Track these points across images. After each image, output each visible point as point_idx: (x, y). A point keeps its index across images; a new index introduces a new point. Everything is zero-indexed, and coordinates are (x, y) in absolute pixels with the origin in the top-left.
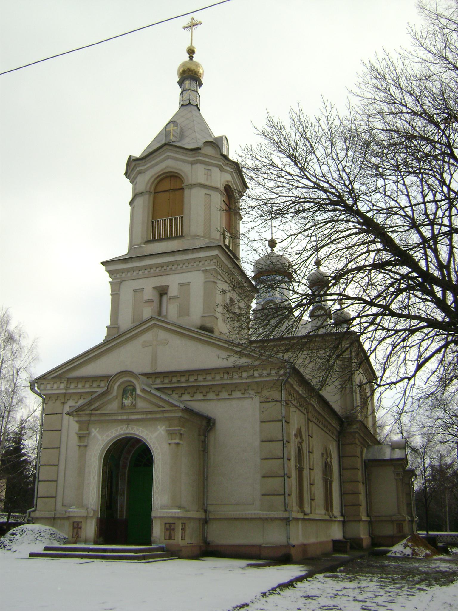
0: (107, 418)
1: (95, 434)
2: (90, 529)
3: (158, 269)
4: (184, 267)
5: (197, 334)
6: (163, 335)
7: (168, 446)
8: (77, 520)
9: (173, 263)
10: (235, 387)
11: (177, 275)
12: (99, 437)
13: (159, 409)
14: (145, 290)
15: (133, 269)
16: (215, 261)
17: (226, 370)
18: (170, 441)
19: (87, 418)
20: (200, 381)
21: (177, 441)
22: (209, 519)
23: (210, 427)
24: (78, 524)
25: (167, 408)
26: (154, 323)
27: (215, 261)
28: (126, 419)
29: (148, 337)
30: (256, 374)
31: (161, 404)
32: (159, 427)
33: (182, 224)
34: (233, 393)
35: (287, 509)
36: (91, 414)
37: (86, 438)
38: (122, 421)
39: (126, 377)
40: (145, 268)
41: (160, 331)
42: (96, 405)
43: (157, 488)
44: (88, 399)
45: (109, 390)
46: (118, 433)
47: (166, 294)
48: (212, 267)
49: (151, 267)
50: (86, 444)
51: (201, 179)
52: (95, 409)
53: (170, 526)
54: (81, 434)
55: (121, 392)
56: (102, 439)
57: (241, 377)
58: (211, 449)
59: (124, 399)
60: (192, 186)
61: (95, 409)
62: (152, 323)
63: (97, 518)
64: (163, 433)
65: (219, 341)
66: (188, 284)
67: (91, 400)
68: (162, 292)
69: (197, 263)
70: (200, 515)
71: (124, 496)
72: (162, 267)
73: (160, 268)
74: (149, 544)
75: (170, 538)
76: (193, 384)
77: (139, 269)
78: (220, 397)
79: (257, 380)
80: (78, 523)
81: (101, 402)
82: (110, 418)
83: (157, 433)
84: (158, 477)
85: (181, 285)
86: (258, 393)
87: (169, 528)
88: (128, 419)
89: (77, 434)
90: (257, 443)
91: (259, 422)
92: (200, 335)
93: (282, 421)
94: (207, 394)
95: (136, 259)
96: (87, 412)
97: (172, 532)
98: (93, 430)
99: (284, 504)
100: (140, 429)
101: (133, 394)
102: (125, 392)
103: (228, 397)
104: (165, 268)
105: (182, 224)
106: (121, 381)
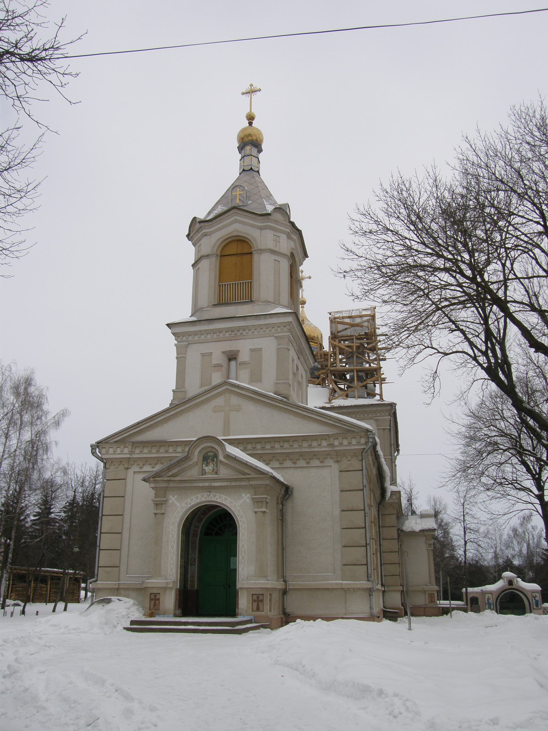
0: (187, 485)
1: (173, 501)
2: (169, 601)
3: (227, 334)
4: (256, 333)
5: (273, 401)
6: (235, 400)
7: (254, 514)
8: (155, 591)
9: (244, 328)
10: (315, 455)
11: (248, 340)
12: (178, 505)
13: (244, 477)
14: (213, 355)
15: (201, 333)
16: (288, 327)
17: (304, 438)
18: (256, 510)
19: (164, 485)
20: (277, 449)
21: (264, 509)
22: (289, 589)
23: (288, 496)
24: (155, 596)
25: (253, 475)
26: (227, 388)
27: (288, 327)
28: (208, 486)
29: (220, 401)
30: (336, 443)
31: (247, 471)
32: (243, 495)
33: (251, 289)
34: (298, 462)
35: (370, 579)
36: (169, 481)
37: (164, 506)
38: (203, 488)
39: (207, 442)
40: (214, 331)
41: (233, 396)
42: (174, 471)
43: (243, 558)
44: (166, 465)
45: (189, 456)
46: (198, 501)
47: (235, 359)
48: (286, 334)
49: (220, 331)
50: (163, 511)
51: (271, 245)
52: (173, 476)
53: (258, 597)
54: (157, 501)
55: (201, 458)
56: (180, 507)
57: (311, 445)
58: (289, 518)
59: (204, 466)
60: (261, 251)
61: (173, 476)
62: (224, 388)
63: (176, 589)
64: (248, 501)
65: (297, 409)
66: (260, 350)
67: (170, 465)
68: (232, 357)
69: (270, 329)
70: (280, 585)
71: (194, 565)
72: (232, 331)
73: (230, 333)
74: (234, 614)
75: (258, 609)
76: (269, 452)
77: (208, 332)
78: (297, 466)
79: (337, 448)
80: (155, 594)
81: (180, 468)
82: (187, 485)
83: (242, 501)
84: (243, 546)
85: (252, 350)
86: (338, 461)
87: (258, 600)
88: (210, 486)
89: (153, 501)
90: (337, 512)
91: (339, 492)
92: (276, 402)
93: (363, 490)
94: (284, 462)
95: (204, 322)
96: (166, 479)
97: (260, 604)
98: (171, 497)
99: (366, 574)
100: (223, 497)
101: (214, 461)
102: (206, 459)
103: (305, 465)
104: (236, 332)
105: (251, 289)
106: (202, 446)
